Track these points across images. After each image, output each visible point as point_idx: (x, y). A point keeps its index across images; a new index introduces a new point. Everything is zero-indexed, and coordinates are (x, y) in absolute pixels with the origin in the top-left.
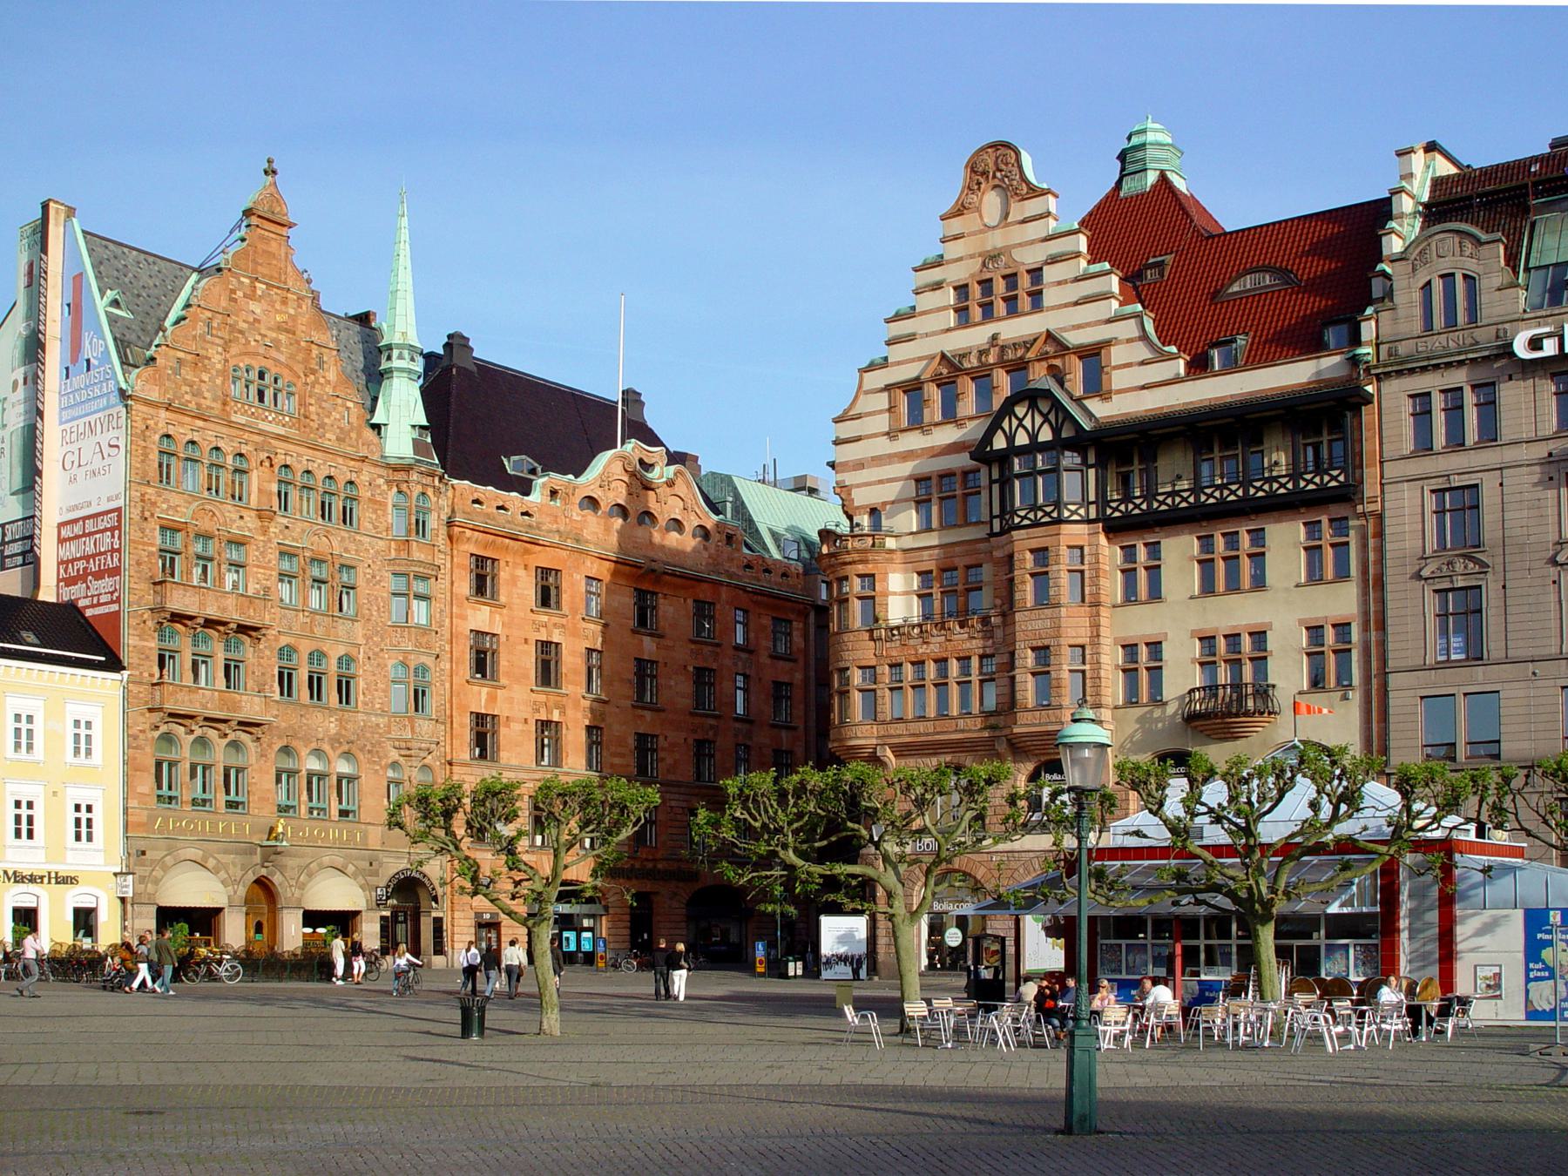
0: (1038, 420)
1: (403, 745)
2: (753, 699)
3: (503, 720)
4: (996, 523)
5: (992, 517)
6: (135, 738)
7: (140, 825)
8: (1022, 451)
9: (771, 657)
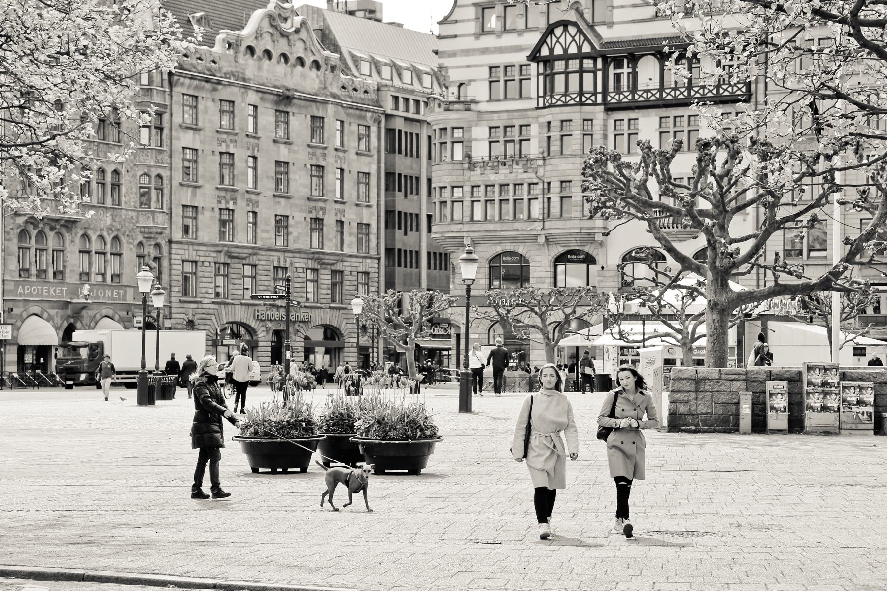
0: (569, 39)
1: (147, 230)
2: (346, 187)
3: (200, 209)
4: (541, 100)
5: (538, 97)
6: (8, 233)
7: (11, 291)
8: (559, 58)
9: (357, 154)
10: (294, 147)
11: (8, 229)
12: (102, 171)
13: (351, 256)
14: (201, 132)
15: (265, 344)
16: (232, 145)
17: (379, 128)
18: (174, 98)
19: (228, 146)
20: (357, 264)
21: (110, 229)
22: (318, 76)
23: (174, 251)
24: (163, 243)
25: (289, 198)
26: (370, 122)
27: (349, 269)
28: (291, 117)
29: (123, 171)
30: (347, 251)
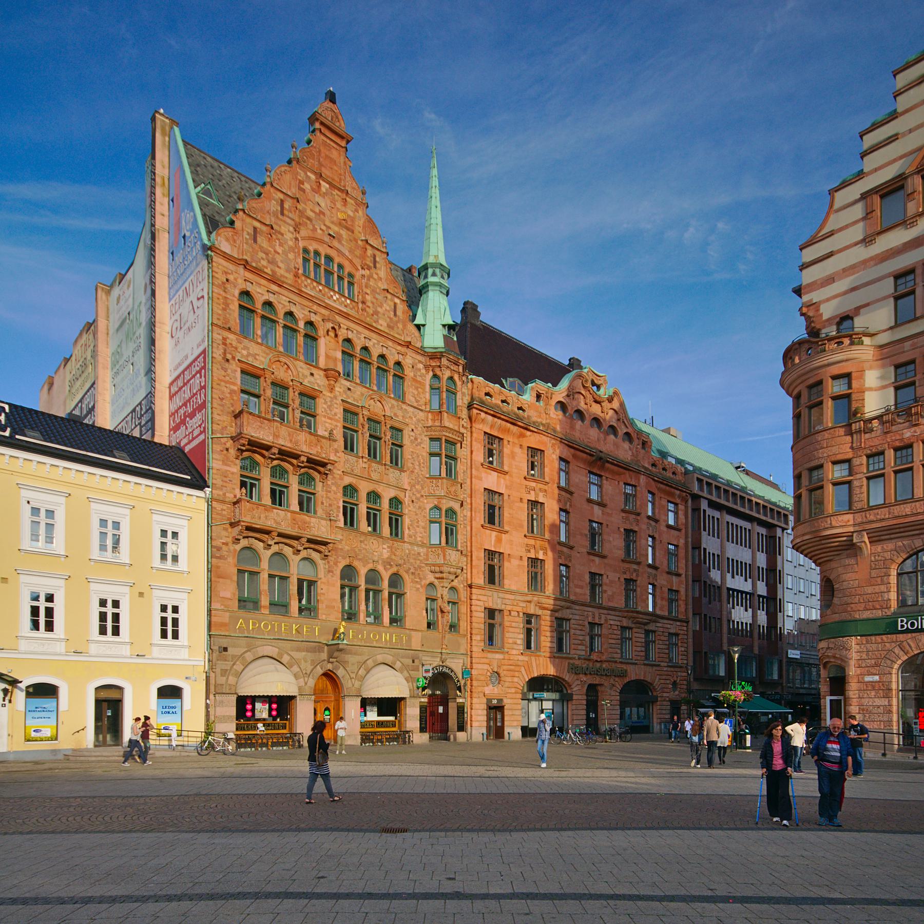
1: (437, 569)
2: (657, 554)
3: (506, 556)
7: (223, 625)
10: (608, 510)
11: (218, 543)
12: (374, 496)
13: (663, 618)
14: (507, 477)
15: (580, 697)
16: (541, 494)
17: (686, 507)
18: (474, 435)
19: (537, 495)
20: (669, 626)
21: (387, 563)
22: (630, 449)
23: (474, 597)
24: (461, 587)
25: (604, 557)
26: (678, 501)
27: (661, 630)
28: (605, 482)
29: (407, 500)
30: (658, 612)
